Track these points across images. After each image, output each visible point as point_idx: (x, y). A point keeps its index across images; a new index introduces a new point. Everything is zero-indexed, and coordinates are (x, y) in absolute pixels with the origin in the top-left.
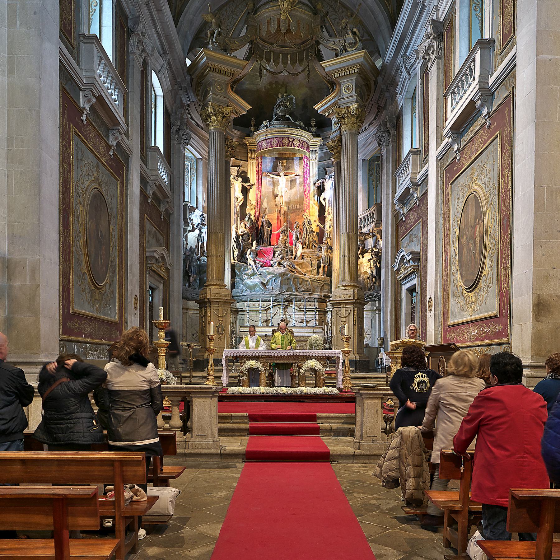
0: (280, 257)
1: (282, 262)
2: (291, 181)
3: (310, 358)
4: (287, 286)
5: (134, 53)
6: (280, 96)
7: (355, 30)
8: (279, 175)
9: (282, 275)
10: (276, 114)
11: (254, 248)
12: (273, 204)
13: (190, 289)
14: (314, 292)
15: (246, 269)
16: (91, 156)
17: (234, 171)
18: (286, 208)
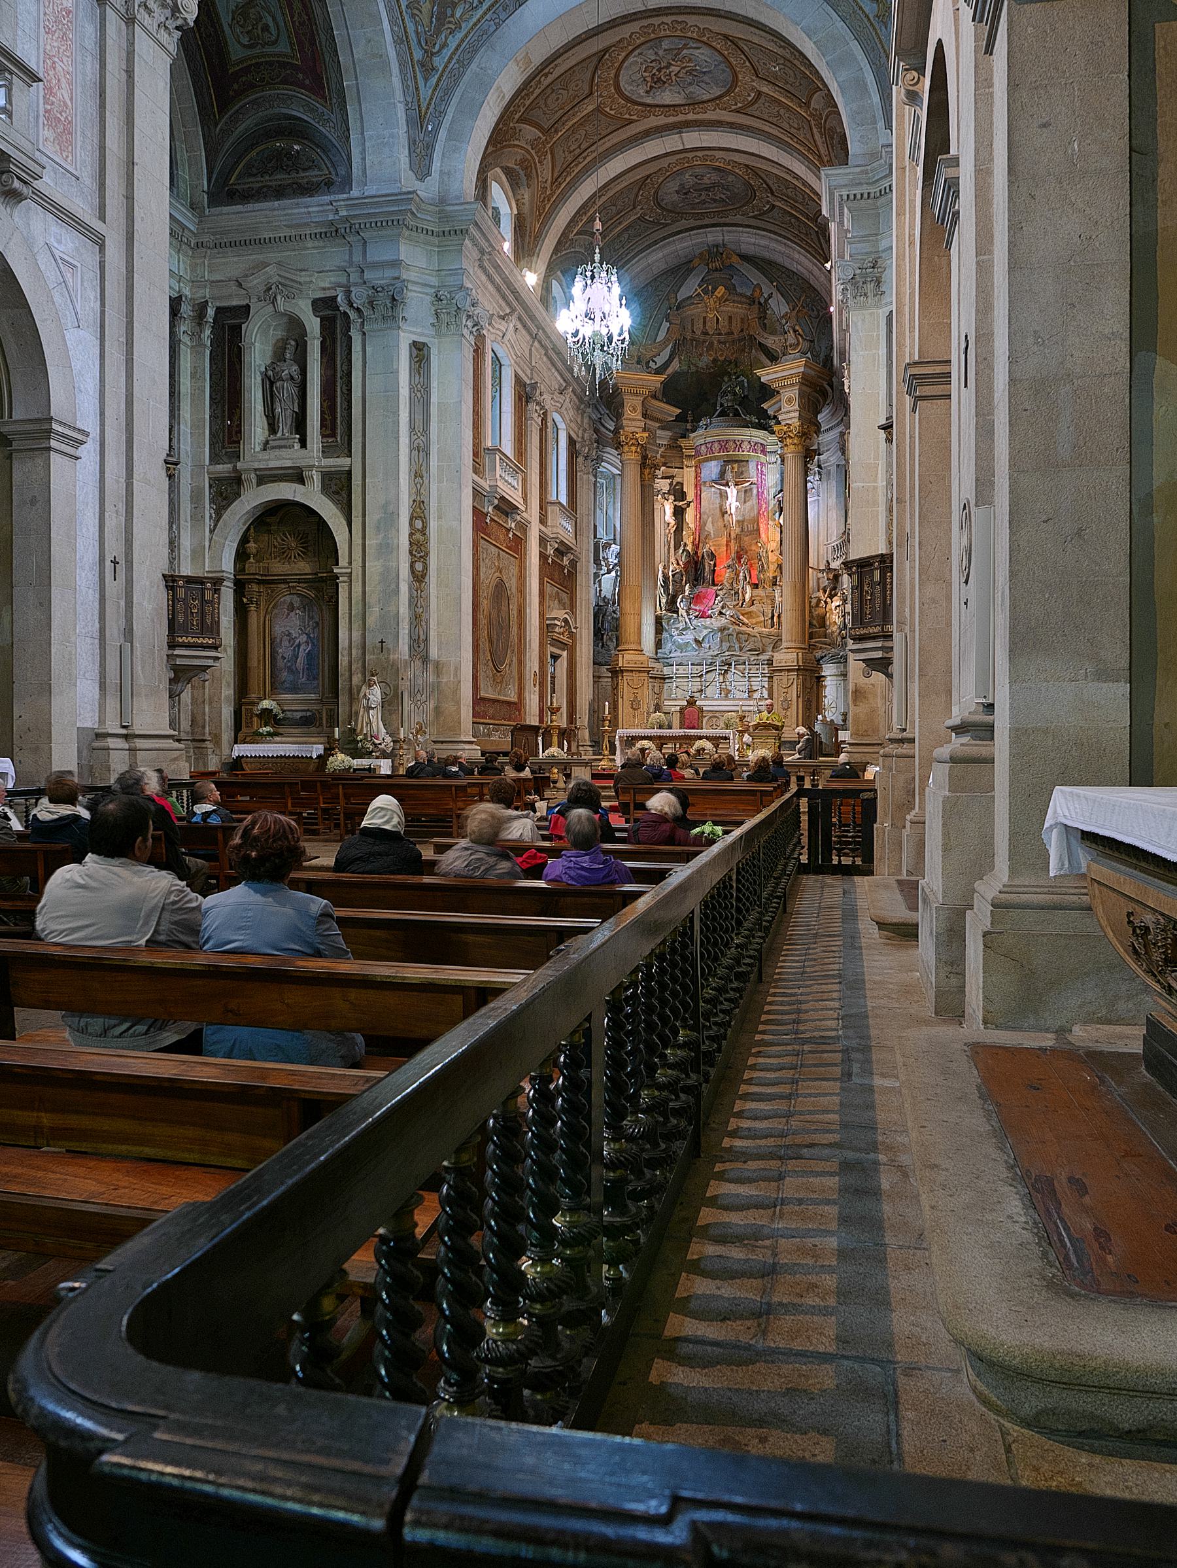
0: (720, 605)
1: (724, 611)
2: (746, 491)
3: (701, 738)
4: (728, 644)
5: (532, 418)
6: (726, 379)
7: (797, 328)
8: (727, 485)
9: (722, 630)
10: (722, 405)
11: (687, 594)
12: (720, 524)
13: (603, 651)
14: (764, 651)
15: (677, 621)
16: (493, 549)
17: (663, 485)
18: (738, 530)
